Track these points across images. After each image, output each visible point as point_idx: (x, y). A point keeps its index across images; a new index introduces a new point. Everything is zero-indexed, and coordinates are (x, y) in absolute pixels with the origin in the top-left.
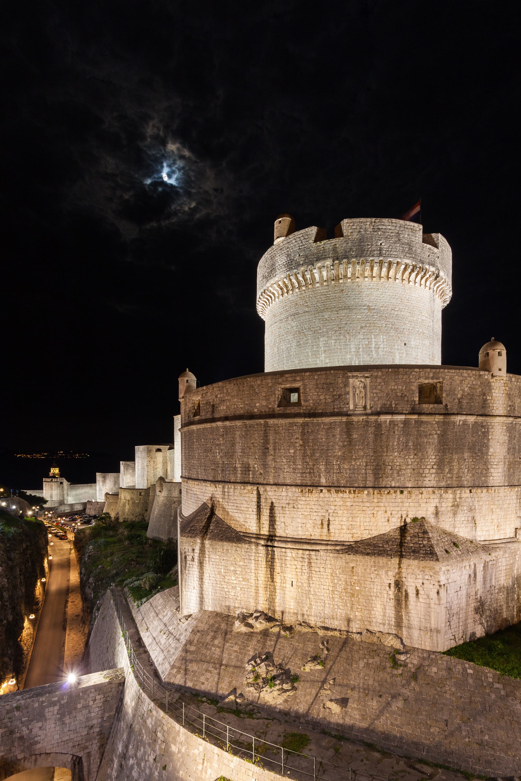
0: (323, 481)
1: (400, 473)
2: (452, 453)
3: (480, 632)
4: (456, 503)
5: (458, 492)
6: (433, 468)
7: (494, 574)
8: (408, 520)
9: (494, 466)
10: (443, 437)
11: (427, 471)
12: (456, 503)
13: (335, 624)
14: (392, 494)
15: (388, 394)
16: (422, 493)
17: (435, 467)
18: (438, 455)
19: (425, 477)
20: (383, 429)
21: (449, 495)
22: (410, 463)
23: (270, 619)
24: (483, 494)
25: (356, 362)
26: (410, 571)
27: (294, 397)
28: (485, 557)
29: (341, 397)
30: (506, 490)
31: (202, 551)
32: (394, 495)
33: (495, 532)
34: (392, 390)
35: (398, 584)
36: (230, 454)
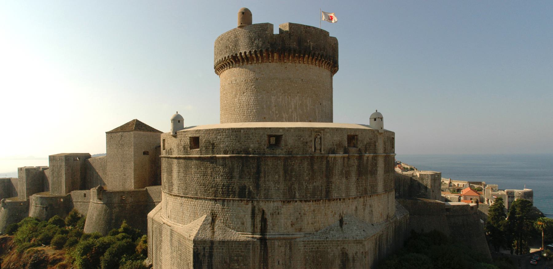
12: (365, 204)
19: (351, 189)
21: (362, 199)
22: (344, 182)
24: (375, 198)
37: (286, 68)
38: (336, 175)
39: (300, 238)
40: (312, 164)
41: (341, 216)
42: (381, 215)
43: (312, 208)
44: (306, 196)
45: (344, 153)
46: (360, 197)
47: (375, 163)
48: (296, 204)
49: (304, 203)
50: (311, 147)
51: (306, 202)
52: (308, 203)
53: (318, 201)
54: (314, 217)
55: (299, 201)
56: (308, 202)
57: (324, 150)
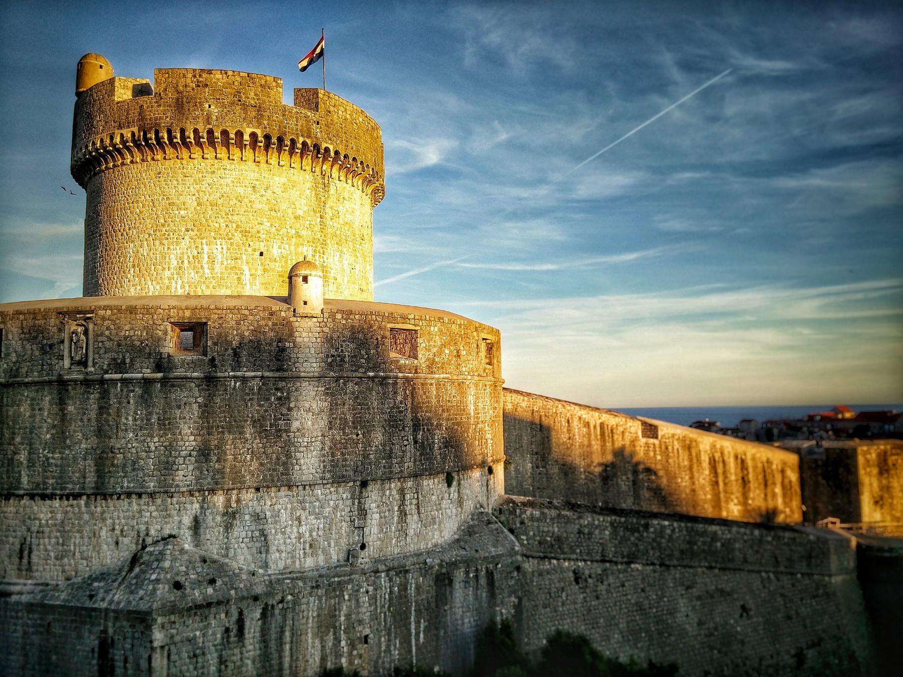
1: (136, 465)
2: (223, 433)
4: (230, 510)
5: (235, 492)
6: (190, 455)
7: (289, 622)
8: (149, 540)
9: (301, 449)
11: (181, 460)
14: (123, 500)
15: (119, 345)
16: (172, 497)
17: (194, 453)
18: (200, 435)
19: (178, 469)
20: (112, 396)
26: (118, 624)
30: (328, 486)
32: (126, 500)
33: (305, 553)
34: (126, 338)
37: (159, 173)
38: (126, 430)
39: (20, 593)
40: (62, 402)
41: (141, 542)
42: (311, 546)
43: (59, 516)
44: (45, 483)
45: (154, 372)
46: (213, 491)
47: (280, 399)
48: (22, 502)
49: (41, 502)
50: (63, 359)
51: (45, 500)
52: (48, 502)
53: (74, 499)
54: (61, 540)
55: (28, 498)
56: (49, 500)
57: (94, 364)
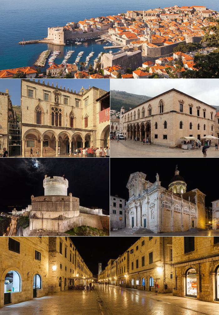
0: (49, 210)
3: (69, 229)
10: (64, 205)
13: (51, 230)
21: (65, 212)
23: (42, 230)
25: (53, 195)
27: (46, 199)
28: (69, 220)
29: (51, 199)
31: (33, 221)
35: (58, 224)
36: (37, 207)
